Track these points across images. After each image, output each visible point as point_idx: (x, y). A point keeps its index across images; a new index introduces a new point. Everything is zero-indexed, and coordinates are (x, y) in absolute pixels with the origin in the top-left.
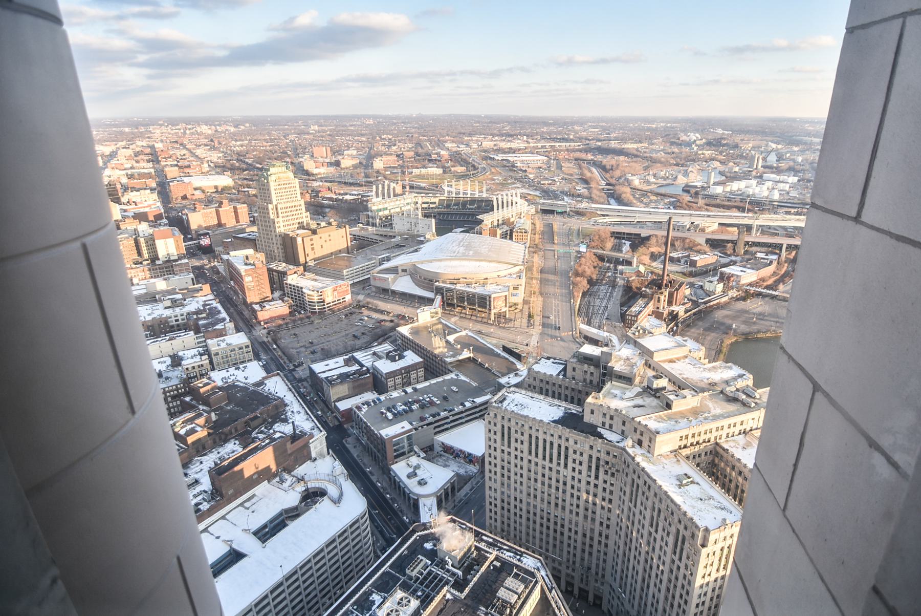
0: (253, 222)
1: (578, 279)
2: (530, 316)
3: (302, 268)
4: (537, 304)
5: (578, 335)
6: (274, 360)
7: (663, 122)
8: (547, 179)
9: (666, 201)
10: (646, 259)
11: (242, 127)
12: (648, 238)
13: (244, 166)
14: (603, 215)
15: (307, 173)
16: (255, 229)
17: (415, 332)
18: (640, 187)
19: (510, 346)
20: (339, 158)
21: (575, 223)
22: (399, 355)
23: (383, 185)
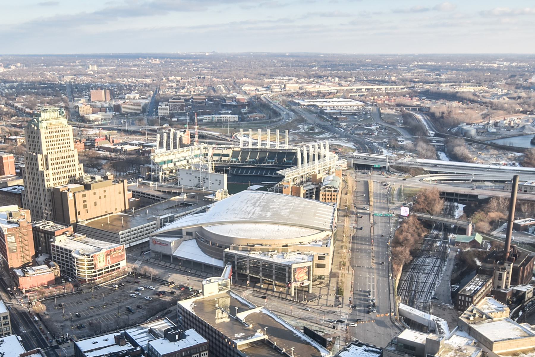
0: (19, 175)
1: (399, 249)
2: (339, 292)
3: (71, 229)
4: (347, 278)
5: (398, 317)
6: (35, 333)
7: (506, 60)
8: (364, 129)
9: (511, 155)
10: (485, 226)
11: (13, 67)
12: (487, 201)
13: (13, 111)
14: (431, 172)
15: (83, 119)
16: (21, 182)
17: (199, 306)
18: (478, 138)
19: (313, 327)
20: (121, 102)
21: (395, 182)
22: (179, 334)
23: (168, 134)
